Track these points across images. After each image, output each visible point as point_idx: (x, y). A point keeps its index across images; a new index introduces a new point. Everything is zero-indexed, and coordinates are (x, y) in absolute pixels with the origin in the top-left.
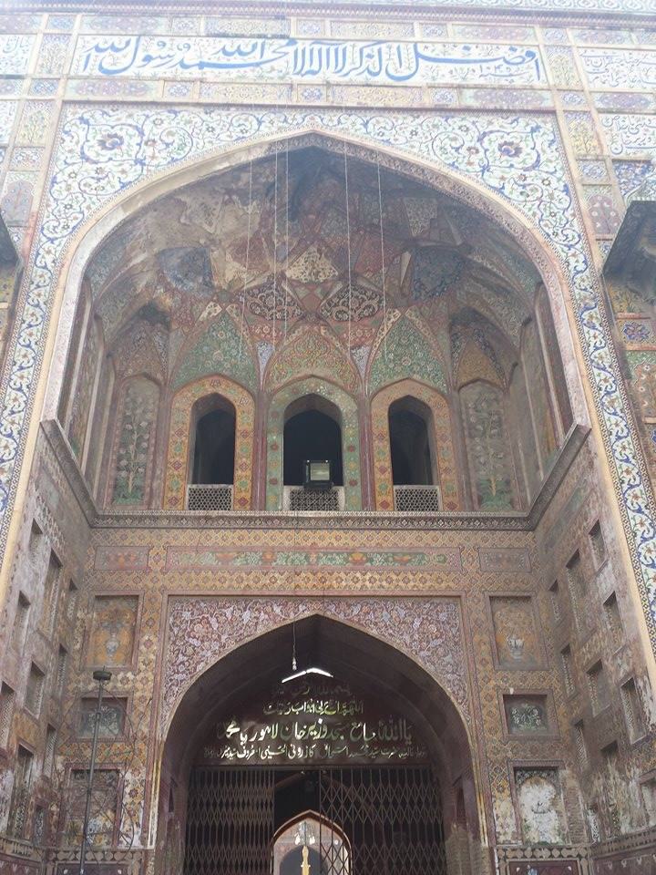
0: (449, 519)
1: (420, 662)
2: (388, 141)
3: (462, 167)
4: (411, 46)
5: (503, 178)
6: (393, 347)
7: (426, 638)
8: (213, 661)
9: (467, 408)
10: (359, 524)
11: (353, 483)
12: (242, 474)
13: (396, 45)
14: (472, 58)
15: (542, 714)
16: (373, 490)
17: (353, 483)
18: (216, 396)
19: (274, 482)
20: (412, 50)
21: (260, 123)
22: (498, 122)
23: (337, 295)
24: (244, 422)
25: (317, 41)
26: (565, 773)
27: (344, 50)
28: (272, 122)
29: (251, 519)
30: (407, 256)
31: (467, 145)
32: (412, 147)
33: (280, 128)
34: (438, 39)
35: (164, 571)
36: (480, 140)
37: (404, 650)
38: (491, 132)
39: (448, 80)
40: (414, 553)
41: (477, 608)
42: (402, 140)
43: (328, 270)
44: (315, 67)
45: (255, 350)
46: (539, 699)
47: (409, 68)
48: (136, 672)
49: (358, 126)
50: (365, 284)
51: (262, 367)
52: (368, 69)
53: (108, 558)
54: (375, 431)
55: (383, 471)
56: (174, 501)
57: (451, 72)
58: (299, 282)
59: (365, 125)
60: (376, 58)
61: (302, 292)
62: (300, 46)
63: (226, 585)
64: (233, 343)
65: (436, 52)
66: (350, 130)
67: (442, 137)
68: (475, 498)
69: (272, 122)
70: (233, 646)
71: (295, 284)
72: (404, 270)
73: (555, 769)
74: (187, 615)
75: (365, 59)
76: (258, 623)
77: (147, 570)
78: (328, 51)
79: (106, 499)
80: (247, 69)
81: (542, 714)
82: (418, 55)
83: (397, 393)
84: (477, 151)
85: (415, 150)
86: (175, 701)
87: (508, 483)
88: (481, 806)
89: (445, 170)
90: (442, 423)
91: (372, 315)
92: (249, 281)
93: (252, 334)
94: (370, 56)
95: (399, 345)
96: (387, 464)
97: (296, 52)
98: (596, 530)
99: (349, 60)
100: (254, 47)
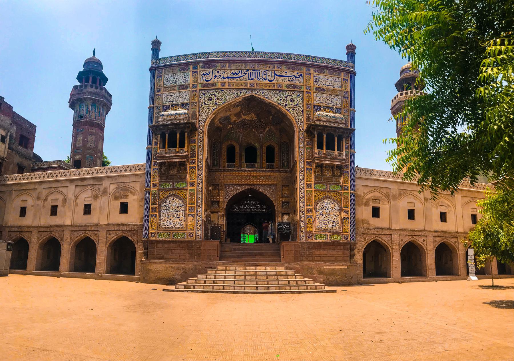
0: (276, 170)
1: (268, 196)
2: (267, 97)
3: (281, 105)
4: (274, 71)
5: (290, 107)
6: (268, 134)
7: (270, 192)
8: (232, 195)
9: (282, 148)
10: (259, 171)
11: (258, 163)
12: (237, 161)
13: (270, 71)
14: (287, 75)
15: (288, 205)
16: (262, 164)
17: (258, 163)
18: (231, 144)
19: (243, 163)
20: (274, 73)
21: (241, 93)
22: (291, 93)
23: (257, 123)
24: (237, 150)
25: (253, 70)
26: (290, 214)
27: (260, 72)
28: (243, 92)
29: (239, 170)
30: (271, 117)
31: (283, 99)
32: (272, 99)
33: (245, 94)
34: (280, 70)
35: (223, 179)
36: (286, 98)
37: (266, 194)
38: (289, 96)
39: (281, 82)
40: (269, 177)
41: (280, 187)
42: (270, 97)
43: (255, 118)
44: (253, 78)
45: (239, 134)
46: (288, 203)
47: (273, 78)
48: (220, 197)
49: (261, 93)
50: (262, 121)
51: (241, 138)
52: (264, 78)
53: (213, 177)
54: (263, 152)
55: (264, 160)
56: (224, 166)
57: (282, 79)
58: (249, 120)
59: (263, 93)
60: (266, 75)
61: (249, 122)
62: (250, 71)
63: (234, 182)
64: (234, 133)
65: (279, 73)
66: (260, 95)
67: (278, 96)
68: (282, 166)
69: (243, 92)
70: (236, 193)
71: (248, 120)
72: (271, 119)
73: (289, 213)
74: (228, 187)
75: (264, 75)
76: (240, 189)
77: (220, 179)
78: (256, 73)
79: (211, 166)
80: (238, 79)
81: (288, 205)
82: (275, 74)
83: (268, 144)
84: (285, 101)
85: (273, 100)
86: (226, 202)
87: (288, 163)
88: (276, 219)
89: (278, 105)
90: (277, 150)
91: (264, 127)
92: (238, 121)
93: (239, 131)
94: (265, 74)
95: (269, 133)
96: (265, 159)
97: (249, 73)
98: (296, 177)
99: (260, 76)
100: (239, 72)
